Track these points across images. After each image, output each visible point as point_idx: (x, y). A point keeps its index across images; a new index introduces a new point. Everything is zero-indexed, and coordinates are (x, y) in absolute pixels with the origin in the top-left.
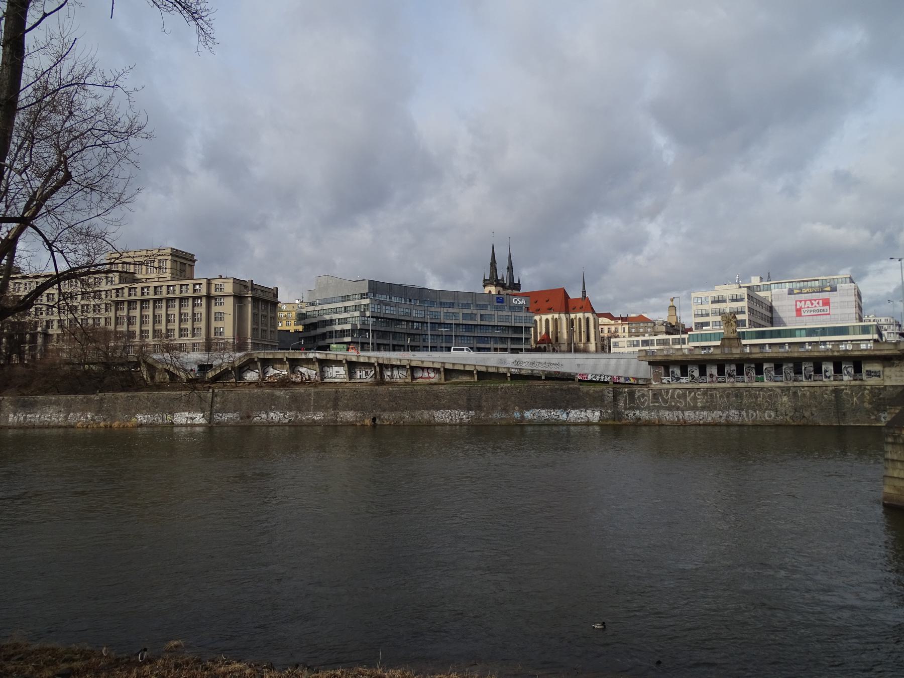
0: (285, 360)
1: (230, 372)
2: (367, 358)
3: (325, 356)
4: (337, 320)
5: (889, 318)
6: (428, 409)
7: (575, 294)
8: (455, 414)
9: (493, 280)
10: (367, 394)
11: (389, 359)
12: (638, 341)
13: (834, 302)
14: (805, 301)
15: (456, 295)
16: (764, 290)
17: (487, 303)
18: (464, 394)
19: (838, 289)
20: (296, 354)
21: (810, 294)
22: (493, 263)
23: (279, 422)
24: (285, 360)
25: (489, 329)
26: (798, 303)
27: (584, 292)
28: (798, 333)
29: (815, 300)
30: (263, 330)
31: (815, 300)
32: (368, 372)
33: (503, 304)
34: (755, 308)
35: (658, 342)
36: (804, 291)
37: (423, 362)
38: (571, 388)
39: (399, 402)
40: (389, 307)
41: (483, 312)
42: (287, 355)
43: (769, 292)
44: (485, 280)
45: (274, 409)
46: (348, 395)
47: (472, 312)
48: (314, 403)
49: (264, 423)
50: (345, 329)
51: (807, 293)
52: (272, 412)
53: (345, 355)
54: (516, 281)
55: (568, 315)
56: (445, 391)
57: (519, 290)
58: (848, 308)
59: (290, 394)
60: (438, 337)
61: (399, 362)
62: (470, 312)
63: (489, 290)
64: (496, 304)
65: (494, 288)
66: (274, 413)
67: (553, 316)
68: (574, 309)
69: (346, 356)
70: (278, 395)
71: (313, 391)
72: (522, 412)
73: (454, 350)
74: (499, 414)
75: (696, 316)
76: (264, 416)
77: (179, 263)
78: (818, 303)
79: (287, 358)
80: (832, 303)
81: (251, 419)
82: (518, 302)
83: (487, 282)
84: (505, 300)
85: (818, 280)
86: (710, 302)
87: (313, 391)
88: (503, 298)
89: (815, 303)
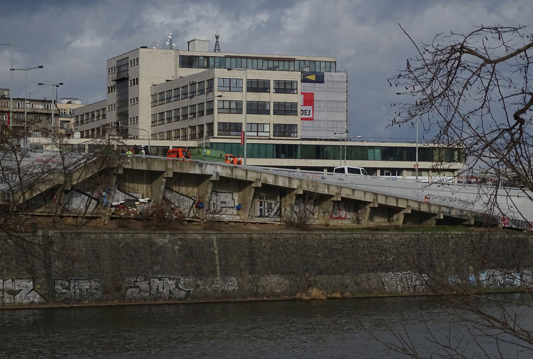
2: (287, 180)
3: (229, 171)
6: (375, 270)
8: (407, 278)
10: (293, 244)
11: (316, 184)
13: (320, 101)
18: (412, 246)
20: (185, 165)
23: (170, 298)
28: (370, 152)
32: (271, 204)
38: (520, 238)
39: (338, 258)
45: (158, 273)
46: (268, 246)
48: (220, 262)
49: (145, 300)
52: (156, 278)
53: (258, 172)
56: (390, 241)
58: (337, 111)
59: (179, 243)
61: (327, 190)
66: (160, 279)
69: (259, 174)
70: (161, 244)
71: (214, 237)
72: (477, 275)
74: (455, 278)
76: (144, 285)
80: (317, 100)
81: (123, 291)
85: (294, 60)
87: (214, 237)
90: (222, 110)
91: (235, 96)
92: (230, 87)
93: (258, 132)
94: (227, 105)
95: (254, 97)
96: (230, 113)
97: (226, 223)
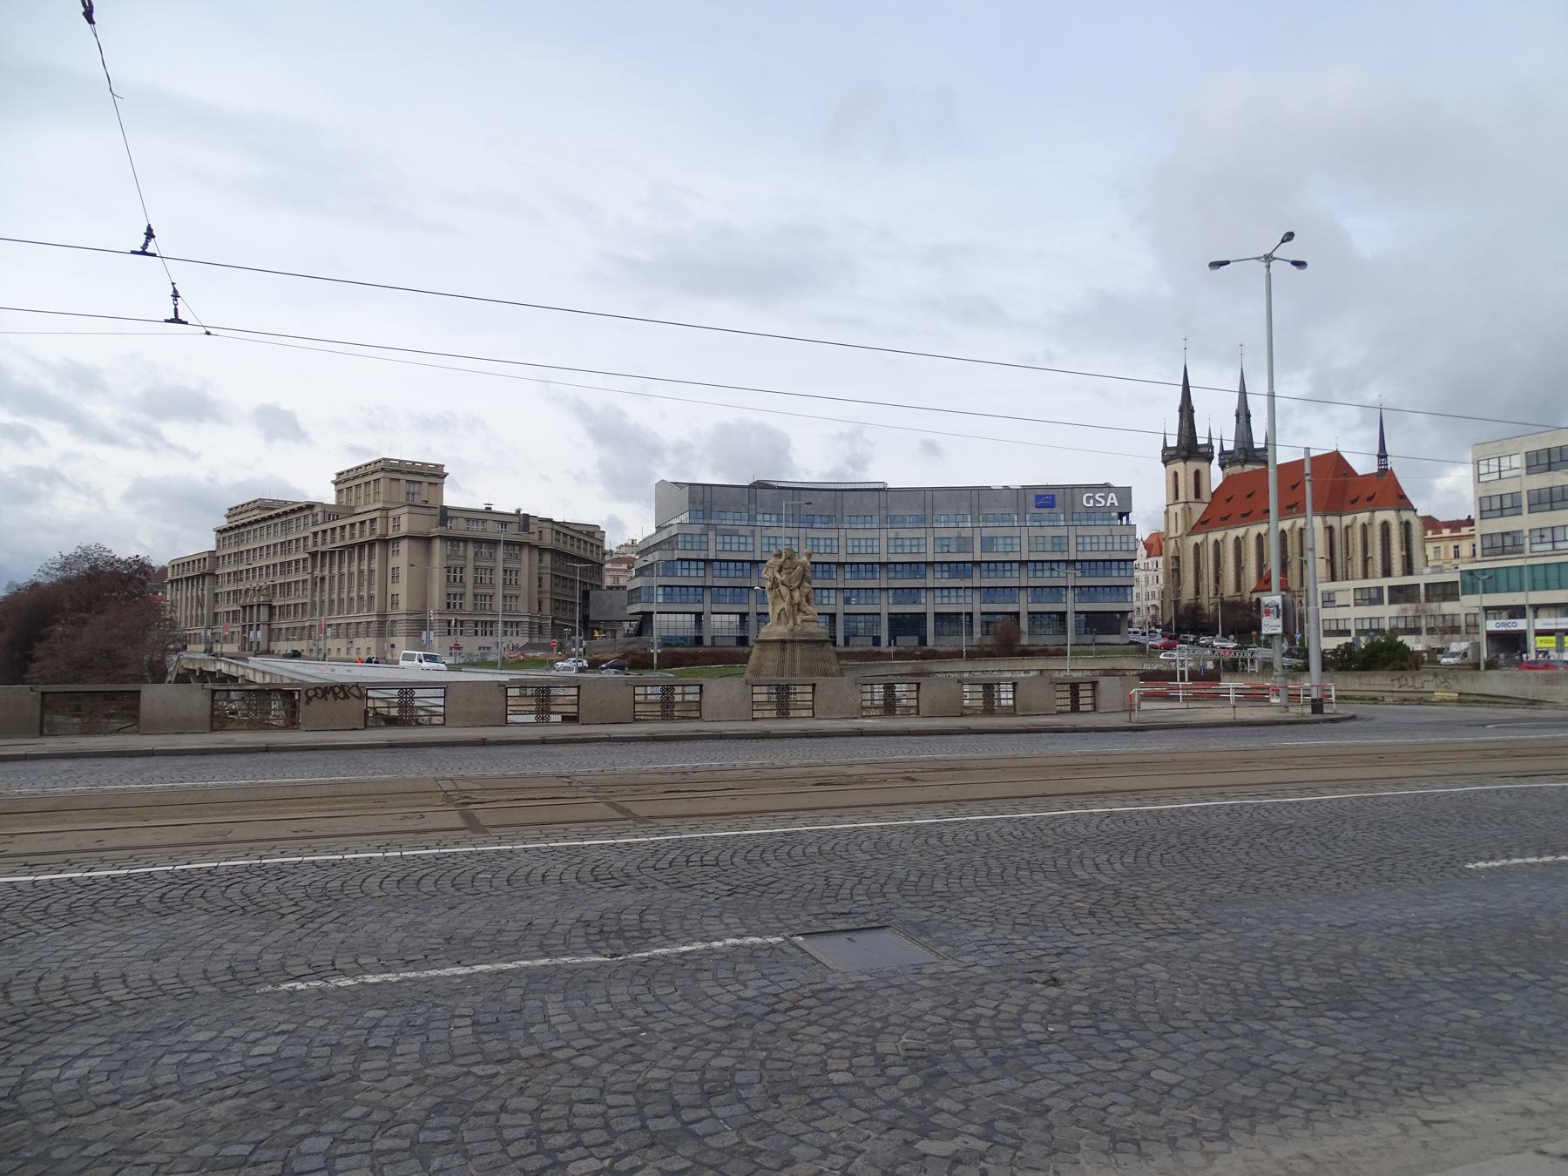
7: (1362, 463)
9: (1187, 449)
12: (1380, 589)
15: (929, 497)
22: (1187, 410)
25: (1042, 570)
27: (1383, 455)
33: (1054, 510)
35: (1326, 598)
40: (735, 539)
44: (1165, 448)
47: (959, 533)
54: (1259, 442)
55: (1333, 520)
60: (839, 592)
64: (1033, 509)
68: (1353, 502)
75: (1485, 515)
77: (403, 483)
82: (1096, 501)
83: (1173, 452)
84: (1058, 501)
88: (1053, 496)
92: (1500, 471)
93: (1554, 542)
94: (1496, 504)
95: (1541, 481)
96: (1502, 516)
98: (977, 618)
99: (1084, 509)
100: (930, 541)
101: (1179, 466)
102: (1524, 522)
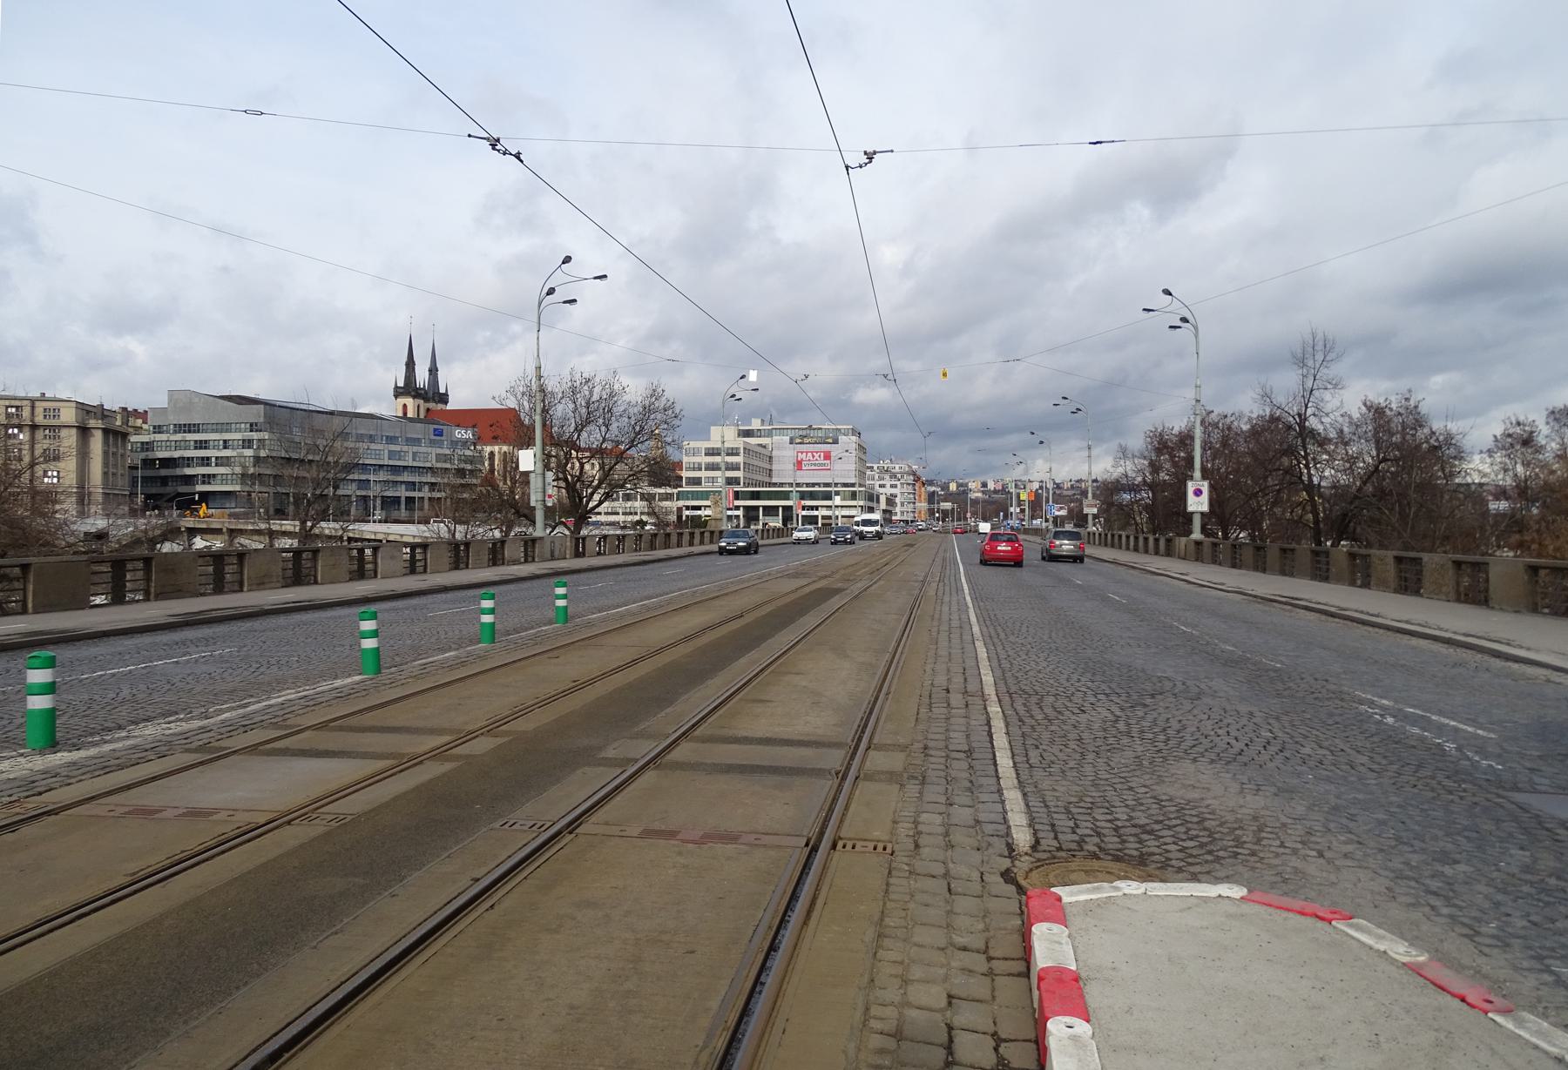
0: (225, 530)
1: (142, 542)
4: (213, 459)
5: (903, 466)
9: (408, 389)
14: (807, 453)
16: (764, 436)
17: (419, 436)
19: (840, 441)
21: (812, 445)
22: (410, 364)
24: (225, 530)
26: (800, 454)
29: (817, 452)
30: (113, 474)
31: (817, 452)
33: (443, 438)
34: (751, 462)
36: (806, 440)
37: (402, 536)
41: (415, 449)
42: (226, 525)
43: (770, 439)
44: (396, 387)
50: (185, 456)
51: (809, 443)
54: (442, 390)
57: (446, 402)
62: (399, 449)
63: (402, 403)
64: (433, 437)
65: (411, 400)
67: (501, 449)
73: (434, 522)
78: (820, 456)
79: (227, 529)
83: (401, 391)
85: (821, 429)
86: (703, 454)
89: (816, 455)
90: (688, 469)
91: (697, 459)
94: (692, 466)
97: (813, 543)
98: (403, 499)
99: (455, 439)
100: (386, 451)
101: (409, 401)
102: (703, 474)
